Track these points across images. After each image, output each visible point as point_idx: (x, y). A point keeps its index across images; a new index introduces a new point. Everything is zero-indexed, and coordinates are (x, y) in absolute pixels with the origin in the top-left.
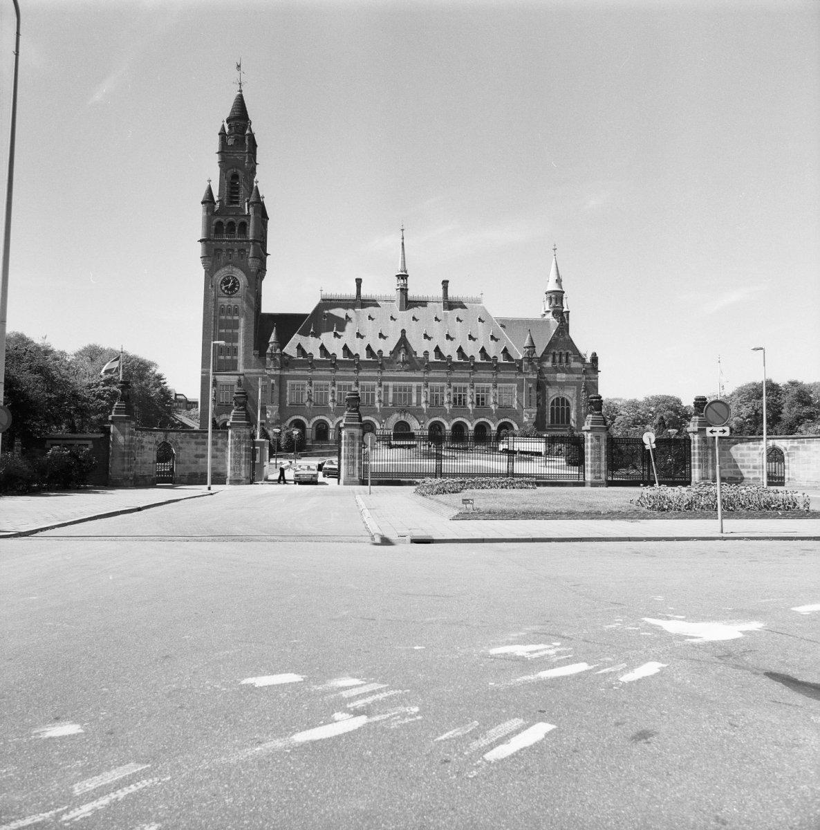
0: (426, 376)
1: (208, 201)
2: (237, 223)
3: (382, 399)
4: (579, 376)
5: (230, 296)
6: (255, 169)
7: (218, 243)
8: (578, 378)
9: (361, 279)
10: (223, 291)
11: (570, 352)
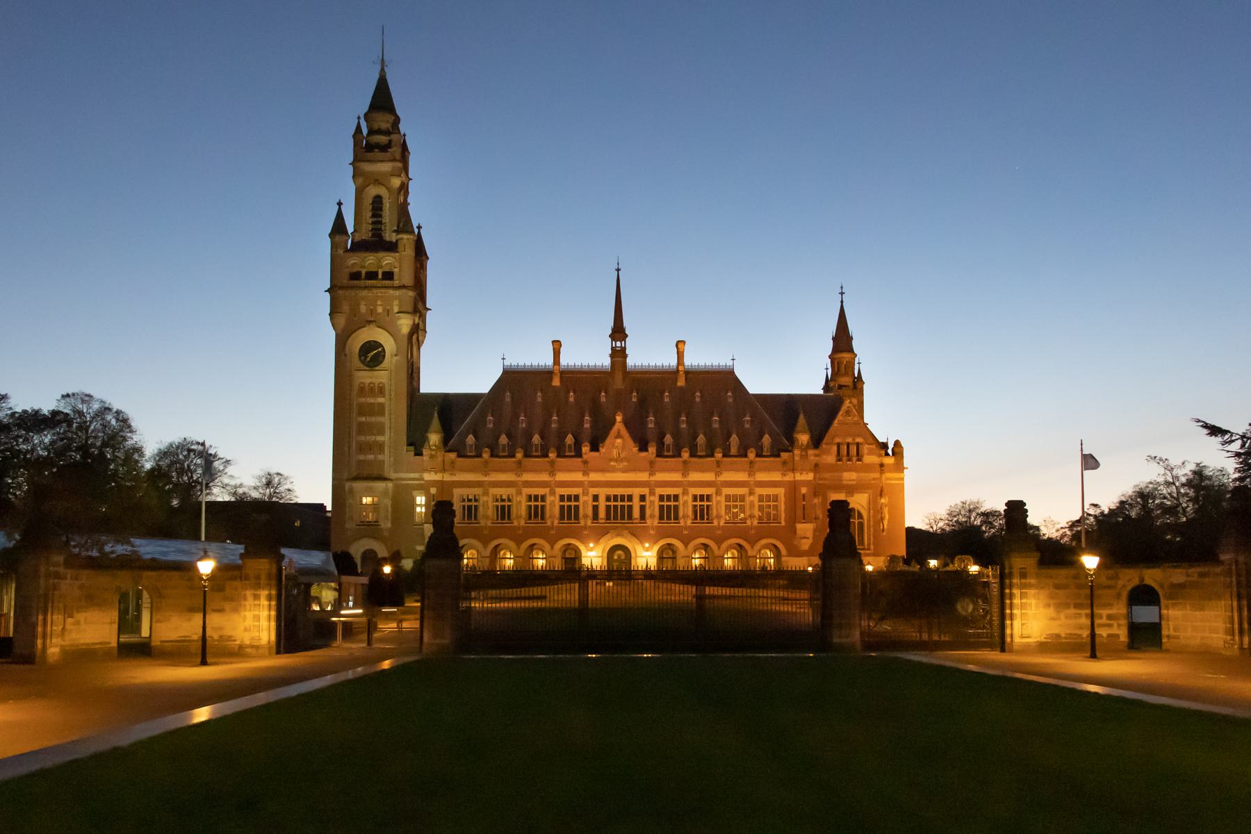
0: (653, 478)
3: (590, 512)
4: (877, 475)
8: (874, 479)
9: (558, 341)
11: (859, 440)
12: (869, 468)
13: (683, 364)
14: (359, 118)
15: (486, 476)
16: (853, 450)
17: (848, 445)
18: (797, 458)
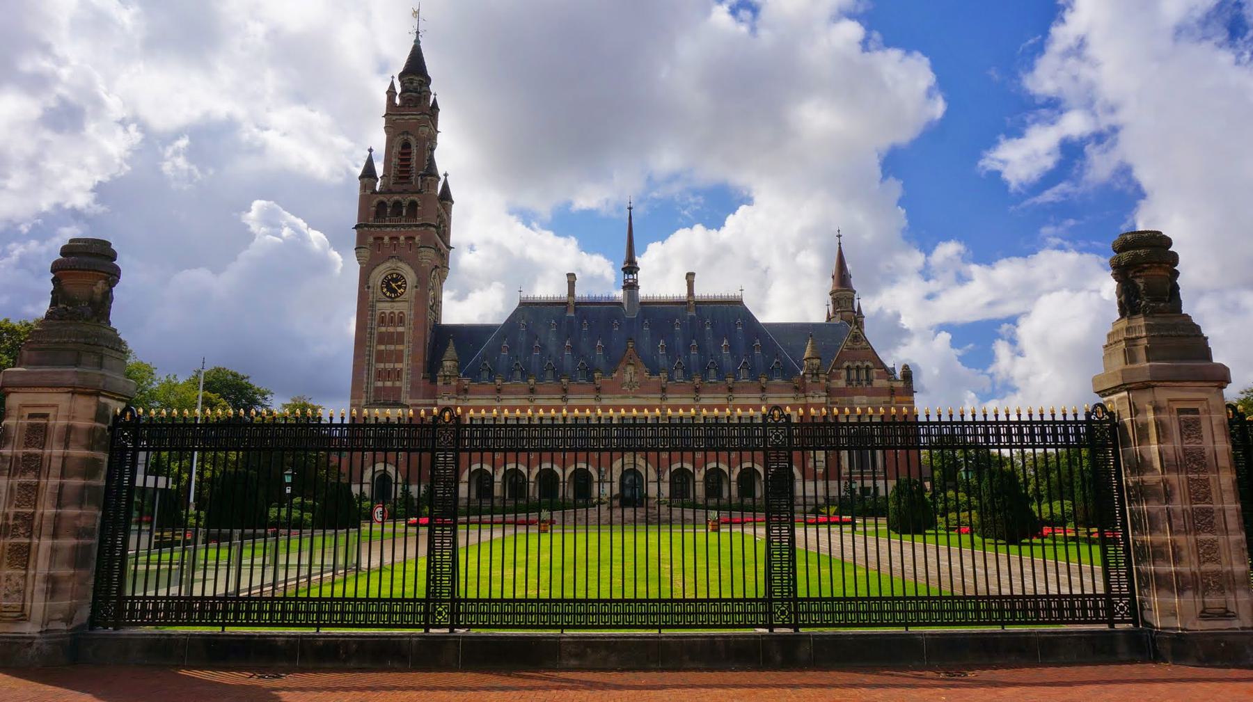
0: (664, 403)
1: (369, 171)
2: (406, 203)
4: (887, 399)
5: (392, 300)
6: (435, 138)
7: (378, 229)
9: (574, 275)
10: (385, 294)
11: (870, 364)
12: (878, 392)
13: (693, 294)
14: (393, 77)
15: (499, 401)
16: (863, 374)
17: (858, 368)
18: (808, 381)
